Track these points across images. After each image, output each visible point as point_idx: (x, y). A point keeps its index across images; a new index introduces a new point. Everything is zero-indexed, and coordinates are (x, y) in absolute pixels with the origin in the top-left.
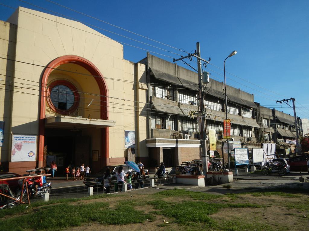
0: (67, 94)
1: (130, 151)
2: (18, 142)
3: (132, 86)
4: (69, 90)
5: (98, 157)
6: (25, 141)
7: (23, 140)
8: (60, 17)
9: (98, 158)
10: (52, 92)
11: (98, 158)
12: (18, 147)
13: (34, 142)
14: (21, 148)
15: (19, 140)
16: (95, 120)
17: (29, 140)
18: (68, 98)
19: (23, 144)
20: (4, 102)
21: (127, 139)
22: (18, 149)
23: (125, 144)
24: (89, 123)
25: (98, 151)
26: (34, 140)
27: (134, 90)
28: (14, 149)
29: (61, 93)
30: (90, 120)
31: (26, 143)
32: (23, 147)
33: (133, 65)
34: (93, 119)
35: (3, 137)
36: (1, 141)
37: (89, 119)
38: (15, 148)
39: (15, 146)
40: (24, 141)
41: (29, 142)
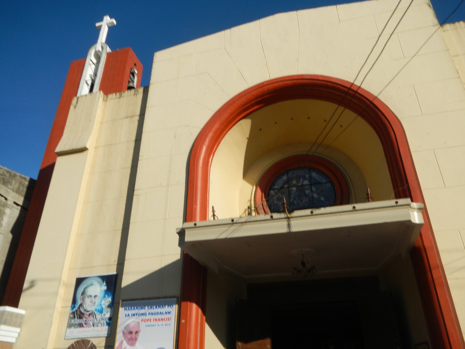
0: (311, 185)
2: (132, 321)
4: (314, 175)
6: (148, 317)
7: (142, 314)
10: (272, 192)
12: (129, 336)
14: (136, 339)
15: (134, 315)
16: (308, 212)
17: (158, 313)
18: (315, 195)
19: (143, 325)
20: (120, 231)
22: (131, 342)
28: (121, 343)
29: (294, 189)
30: (288, 218)
31: (149, 323)
32: (141, 335)
34: (297, 213)
35: (110, 312)
36: (107, 323)
37: (283, 215)
38: (123, 338)
39: (124, 333)
40: (143, 317)
41: (156, 320)
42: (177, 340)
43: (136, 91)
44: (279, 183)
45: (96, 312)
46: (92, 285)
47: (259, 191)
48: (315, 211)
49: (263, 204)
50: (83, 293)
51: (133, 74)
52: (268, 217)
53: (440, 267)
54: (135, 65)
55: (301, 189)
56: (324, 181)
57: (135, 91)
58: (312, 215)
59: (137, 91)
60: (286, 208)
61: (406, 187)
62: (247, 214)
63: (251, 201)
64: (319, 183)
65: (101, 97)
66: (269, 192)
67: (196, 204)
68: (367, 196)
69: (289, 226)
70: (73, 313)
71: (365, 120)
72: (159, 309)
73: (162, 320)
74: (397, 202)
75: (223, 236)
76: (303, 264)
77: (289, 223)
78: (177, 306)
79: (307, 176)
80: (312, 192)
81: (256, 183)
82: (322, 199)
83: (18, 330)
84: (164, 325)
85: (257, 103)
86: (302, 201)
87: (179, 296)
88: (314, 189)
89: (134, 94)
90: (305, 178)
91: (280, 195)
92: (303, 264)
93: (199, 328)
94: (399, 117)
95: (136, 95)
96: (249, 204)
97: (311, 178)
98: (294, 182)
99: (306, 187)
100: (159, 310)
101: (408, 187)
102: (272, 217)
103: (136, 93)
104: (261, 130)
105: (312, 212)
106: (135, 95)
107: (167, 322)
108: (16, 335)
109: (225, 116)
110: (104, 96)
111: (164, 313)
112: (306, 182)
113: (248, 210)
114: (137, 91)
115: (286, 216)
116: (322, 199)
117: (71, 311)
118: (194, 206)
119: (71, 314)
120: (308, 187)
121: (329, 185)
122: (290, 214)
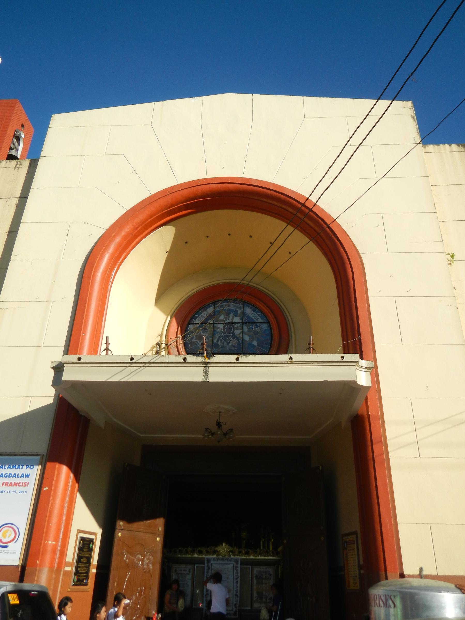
0: (243, 323)
4: (248, 311)
5: (360, 567)
8: (165, 102)
9: (360, 574)
10: (191, 327)
11: (357, 572)
13: (25, 485)
16: (232, 358)
17: (10, 476)
18: (247, 338)
24: (199, 378)
25: (355, 533)
26: (28, 476)
29: (221, 326)
37: (199, 359)
42: (33, 514)
43: (19, 163)
44: (202, 317)
47: (174, 324)
48: (242, 357)
49: (177, 341)
51: (18, 138)
52: (180, 359)
53: (383, 441)
54: (23, 126)
55: (230, 326)
56: (260, 320)
57: (17, 164)
58: (237, 363)
59: (20, 163)
60: (206, 349)
61: (356, 339)
62: (154, 352)
63: (161, 335)
64: (254, 323)
66: (187, 327)
67: (85, 332)
68: (308, 346)
69: (206, 373)
71: (320, 249)
72: (14, 469)
73: (16, 484)
74: (343, 358)
75: (116, 379)
76: (219, 425)
77: (206, 371)
78: (40, 467)
79: (239, 311)
80: (243, 332)
81: (171, 313)
82: (255, 343)
84: (17, 492)
85: (186, 207)
86: (228, 343)
87: (45, 454)
88: (246, 329)
89: (15, 166)
90: (236, 314)
91: (202, 333)
92: (219, 425)
93: (67, 499)
94: (360, 252)
95: (18, 168)
96: (158, 340)
97: (243, 314)
98: (222, 317)
99: (236, 326)
100: (13, 471)
101: (360, 340)
102: (185, 359)
103: (18, 166)
104: (186, 243)
105: (237, 359)
106: (17, 169)
107: (23, 489)
109: (142, 217)
111: (20, 476)
112: (237, 320)
113: (157, 347)
114: (20, 163)
115: (204, 361)
116: (255, 343)
118: (82, 334)
120: (239, 325)
121: (265, 326)
122: (209, 358)
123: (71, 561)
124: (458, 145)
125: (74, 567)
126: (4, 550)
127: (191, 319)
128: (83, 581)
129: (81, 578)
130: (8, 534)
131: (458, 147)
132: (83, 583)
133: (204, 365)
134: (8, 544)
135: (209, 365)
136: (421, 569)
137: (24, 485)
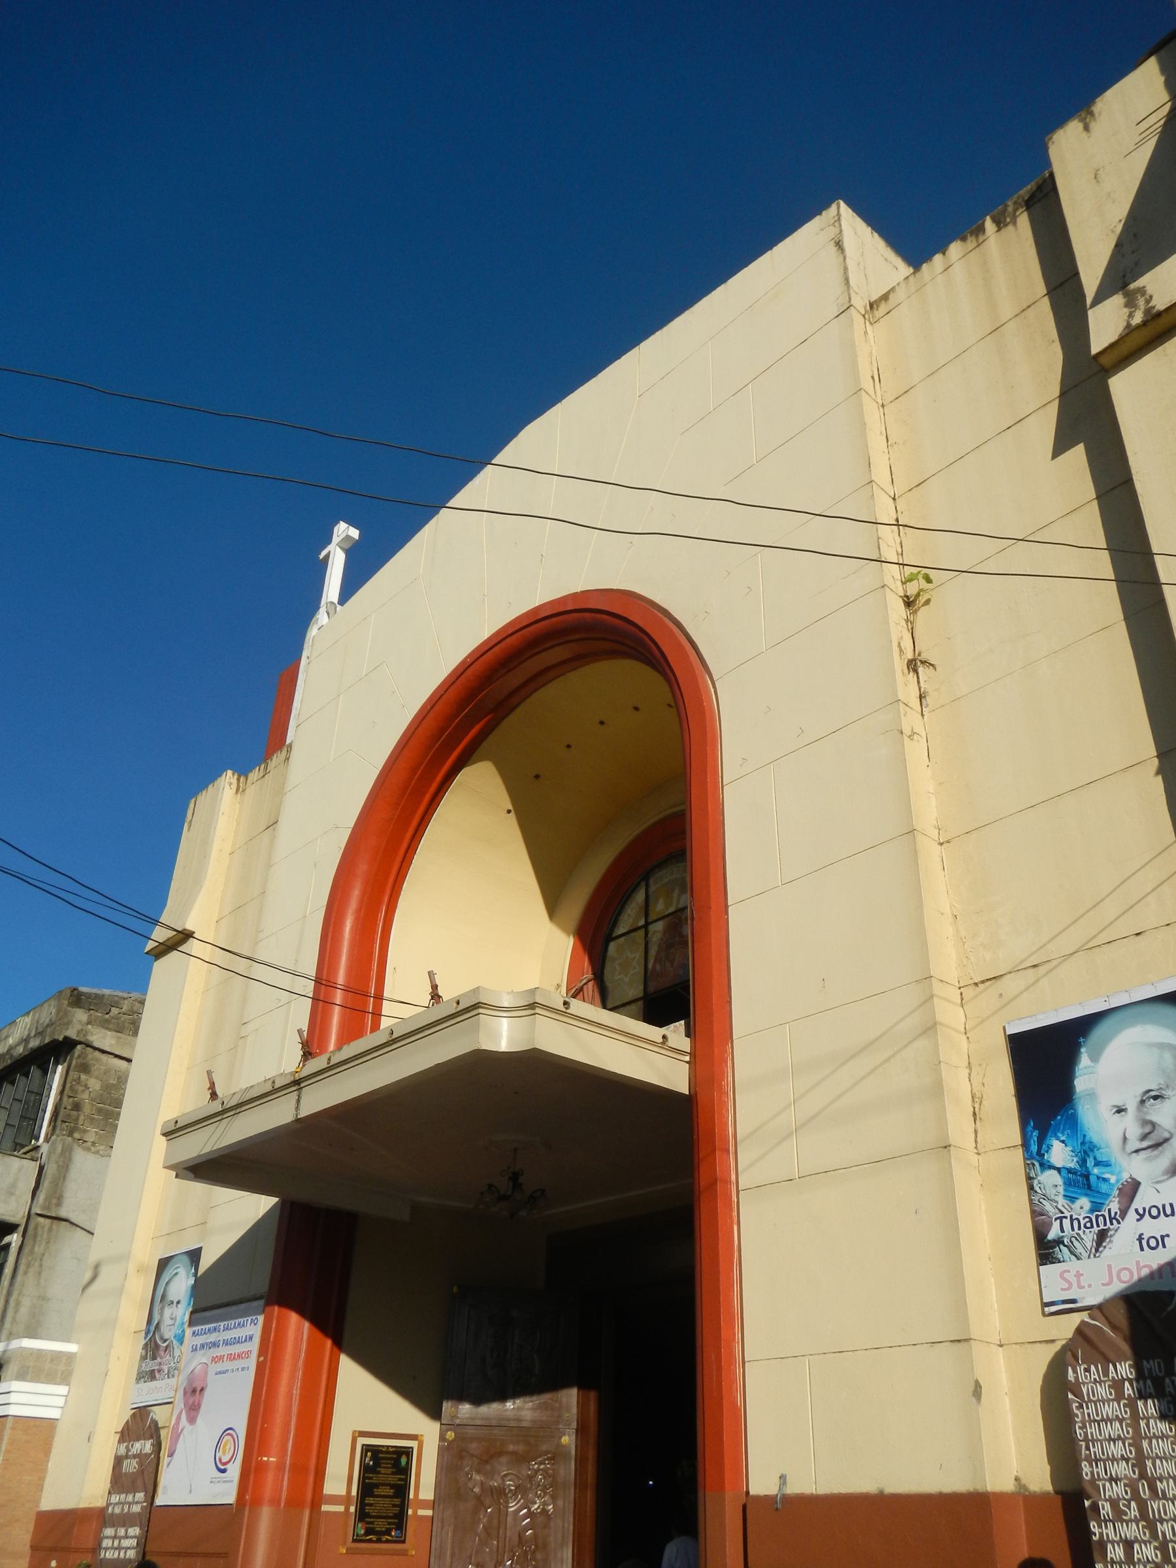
1: (1125, 1369)
3: (1045, 425)
14: (199, 1406)
21: (1060, 1153)
22: (192, 1412)
23: (1046, 1251)
27: (1078, 455)
31: (220, 1367)
33: (1023, 220)
38: (183, 1406)
45: (175, 1342)
46: (176, 1274)
50: (163, 1297)
65: (227, 786)
70: (146, 1345)
83: (63, 1390)
104: (537, 777)
108: (60, 1401)
110: (238, 780)
117: (144, 1342)
119: (143, 1349)
123: (342, 1491)
124: (964, 239)
125: (353, 1505)
126: (223, 1478)
127: (612, 930)
128: (388, 1532)
129: (380, 1525)
130: (228, 1447)
131: (963, 243)
132: (390, 1538)
133: (294, 1088)
134: (227, 1467)
135: (302, 1085)
136: (783, 1478)
137: (247, 1356)
